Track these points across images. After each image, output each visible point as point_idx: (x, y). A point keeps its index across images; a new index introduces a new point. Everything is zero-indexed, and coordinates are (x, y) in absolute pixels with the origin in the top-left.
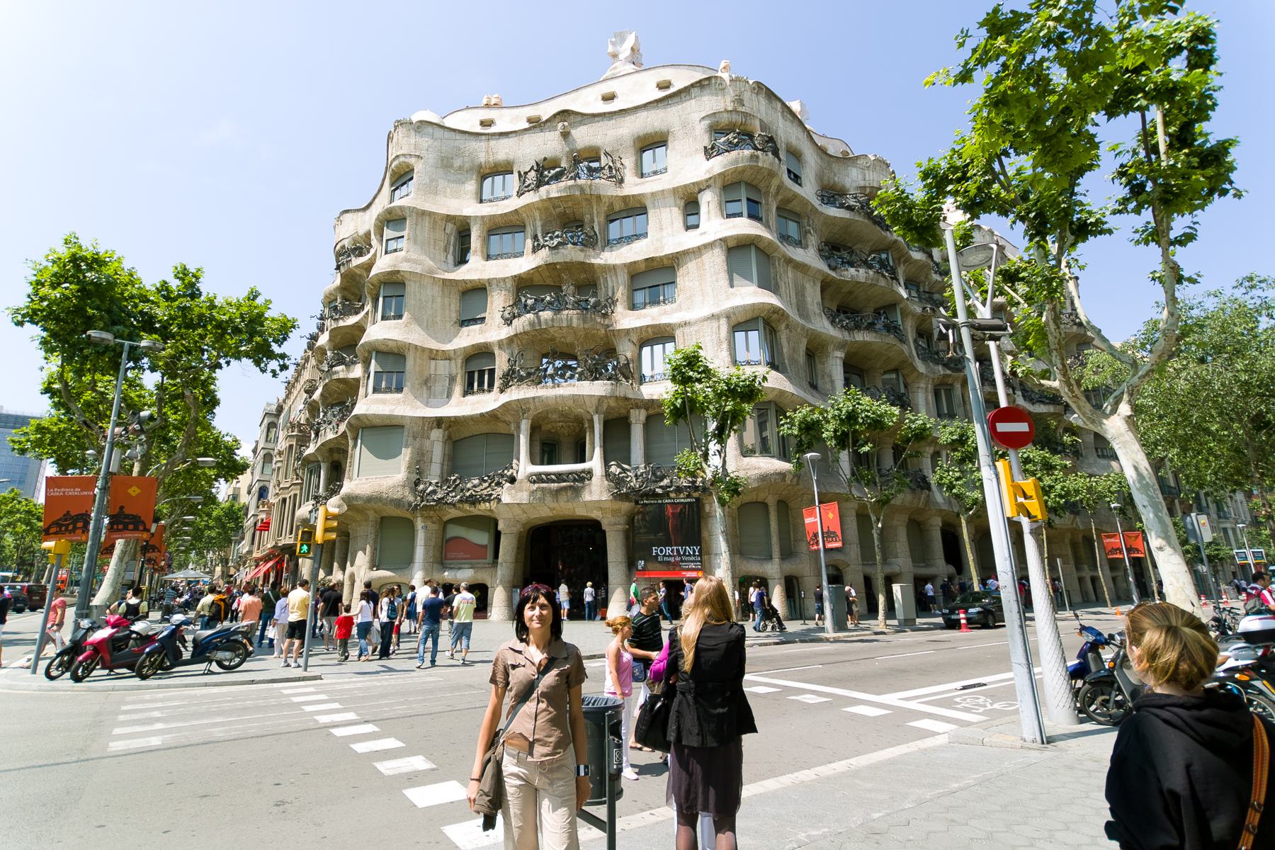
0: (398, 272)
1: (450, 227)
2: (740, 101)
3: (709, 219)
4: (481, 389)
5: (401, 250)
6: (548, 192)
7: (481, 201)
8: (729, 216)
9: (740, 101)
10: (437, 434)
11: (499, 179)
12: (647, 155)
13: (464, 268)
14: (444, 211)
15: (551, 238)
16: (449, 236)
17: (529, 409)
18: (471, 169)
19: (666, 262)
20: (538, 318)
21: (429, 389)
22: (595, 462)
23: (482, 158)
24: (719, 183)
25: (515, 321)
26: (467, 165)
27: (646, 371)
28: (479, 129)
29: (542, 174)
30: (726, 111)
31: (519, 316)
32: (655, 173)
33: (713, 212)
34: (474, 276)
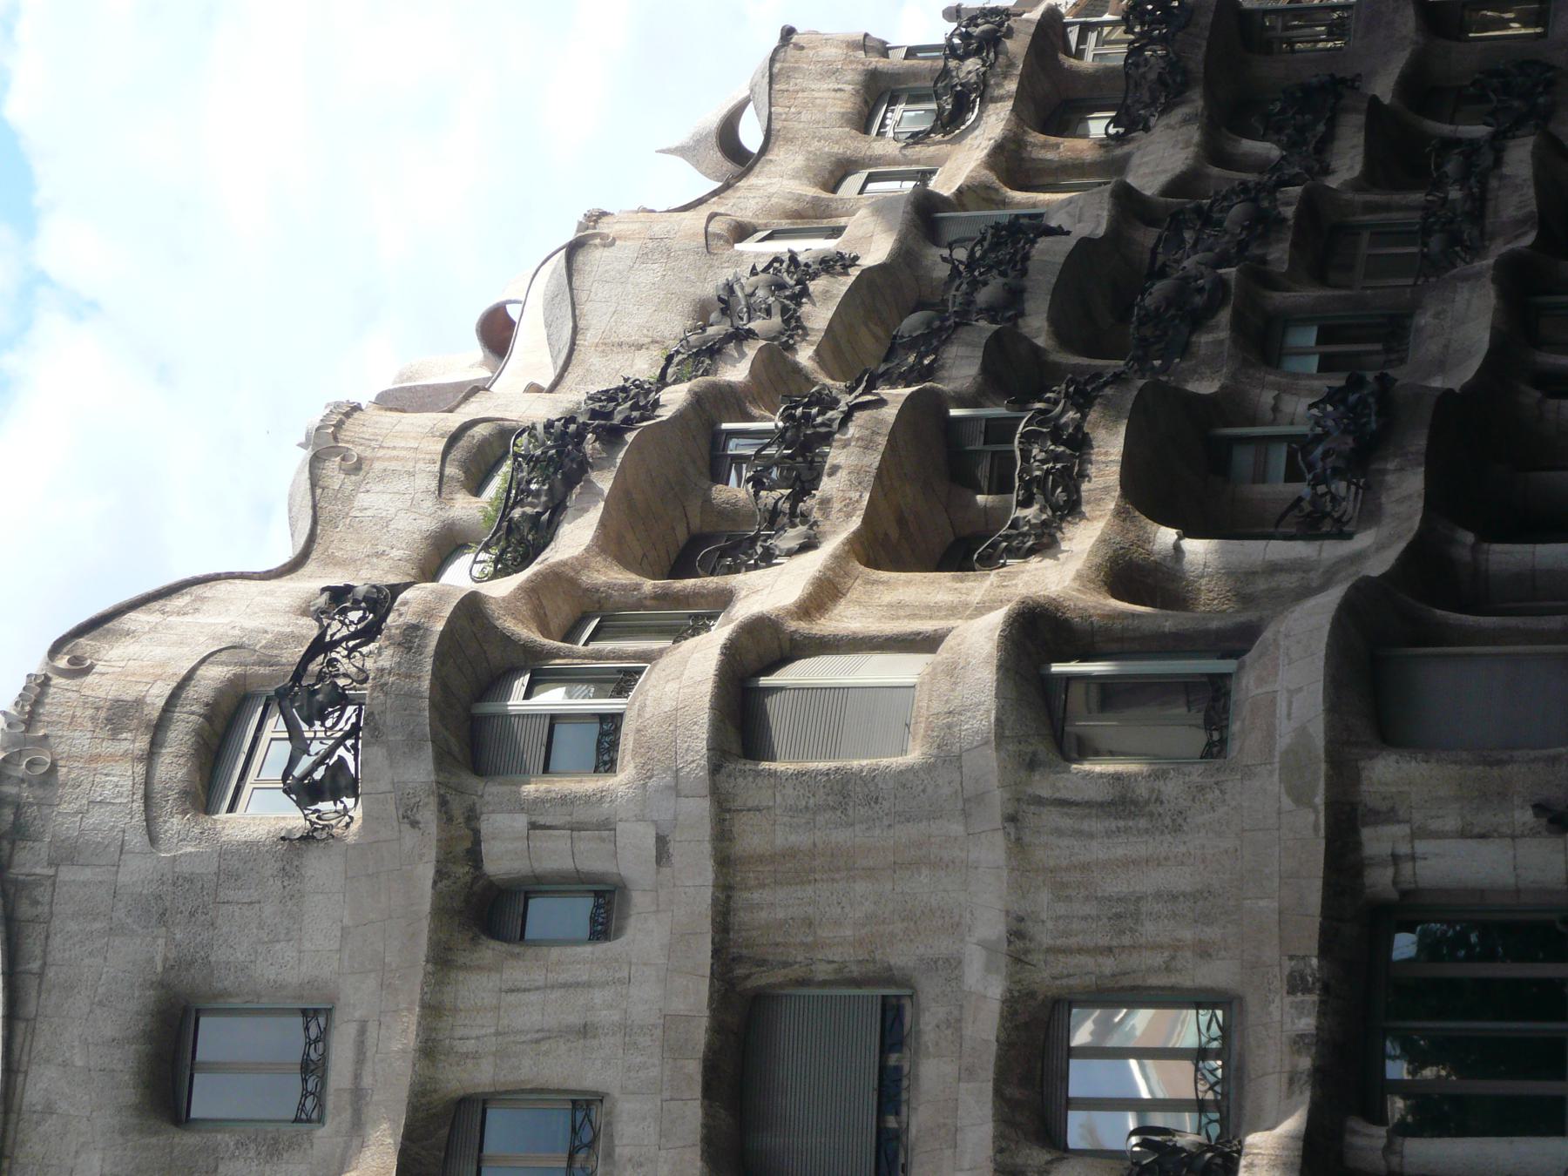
9: (118, 715)
30: (150, 756)
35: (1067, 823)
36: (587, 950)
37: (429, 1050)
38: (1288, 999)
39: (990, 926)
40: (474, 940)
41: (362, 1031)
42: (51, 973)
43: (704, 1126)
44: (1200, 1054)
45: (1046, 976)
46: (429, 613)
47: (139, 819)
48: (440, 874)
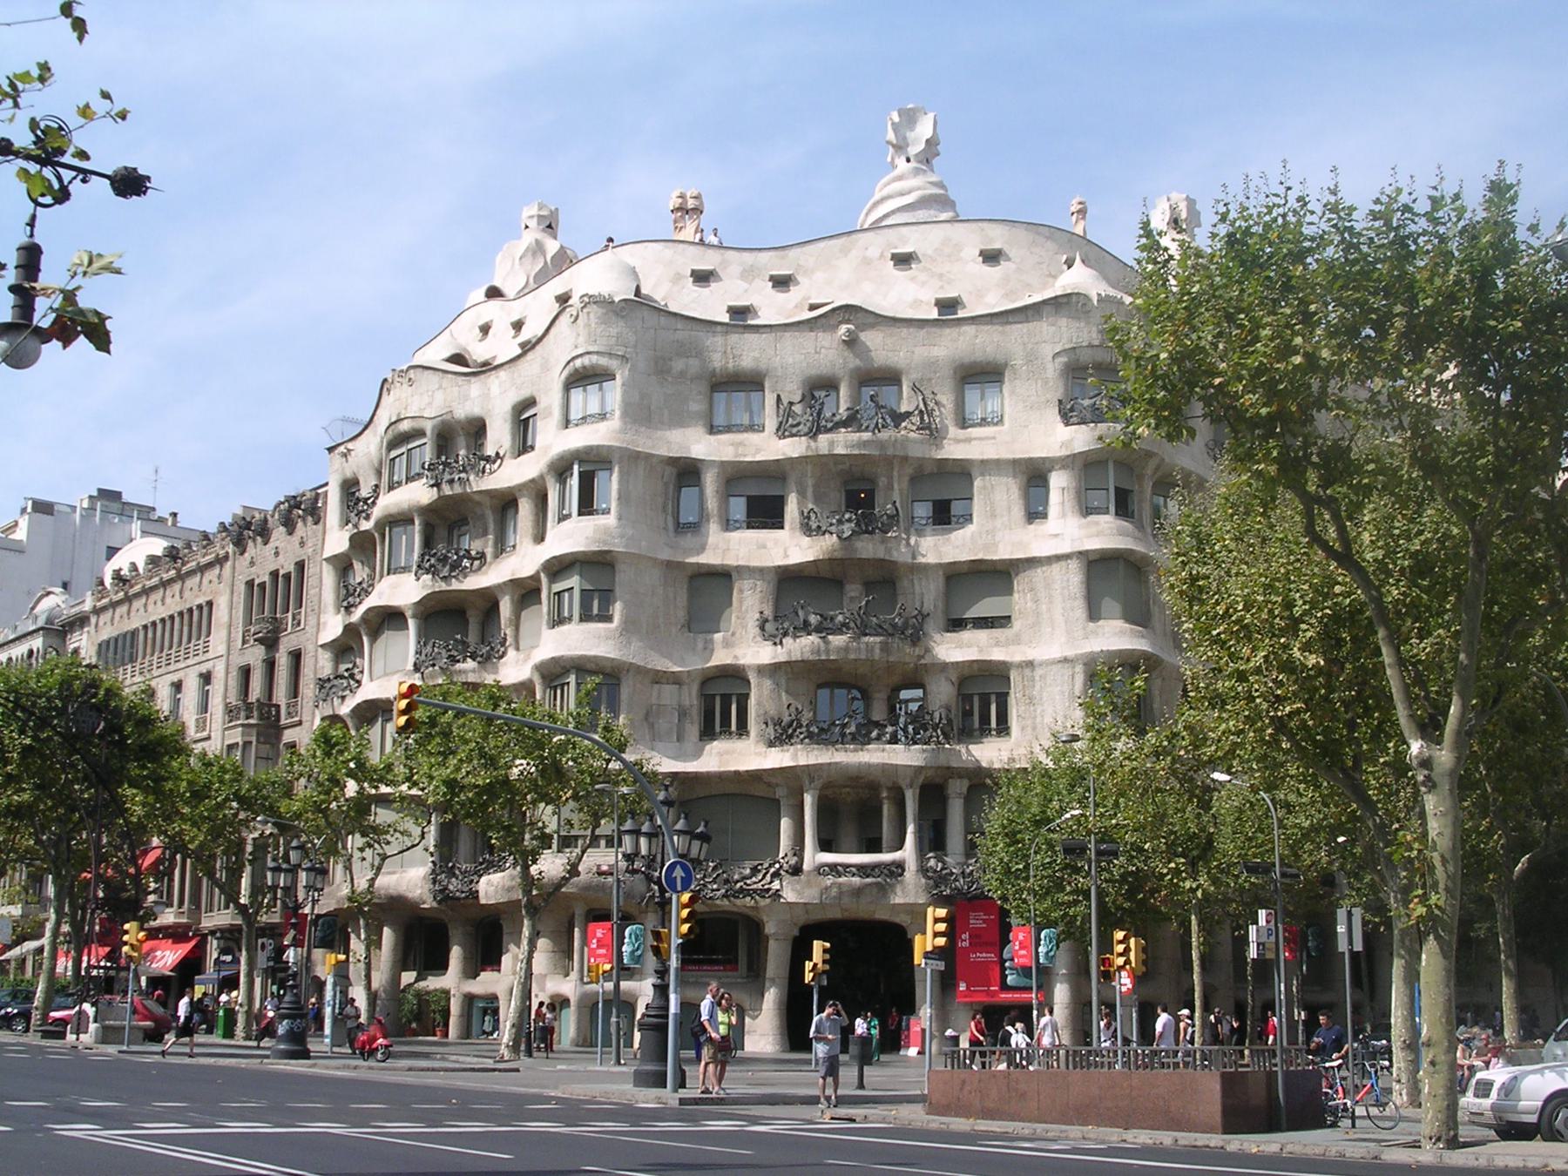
1: (670, 471)
3: (1064, 515)
6: (832, 443)
7: (712, 430)
14: (663, 451)
15: (840, 522)
16: (666, 484)
17: (820, 777)
18: (696, 378)
20: (827, 643)
21: (652, 726)
23: (717, 361)
24: (1079, 464)
25: (788, 641)
30: (1090, 346)
33: (1068, 505)
37: (982, 461)
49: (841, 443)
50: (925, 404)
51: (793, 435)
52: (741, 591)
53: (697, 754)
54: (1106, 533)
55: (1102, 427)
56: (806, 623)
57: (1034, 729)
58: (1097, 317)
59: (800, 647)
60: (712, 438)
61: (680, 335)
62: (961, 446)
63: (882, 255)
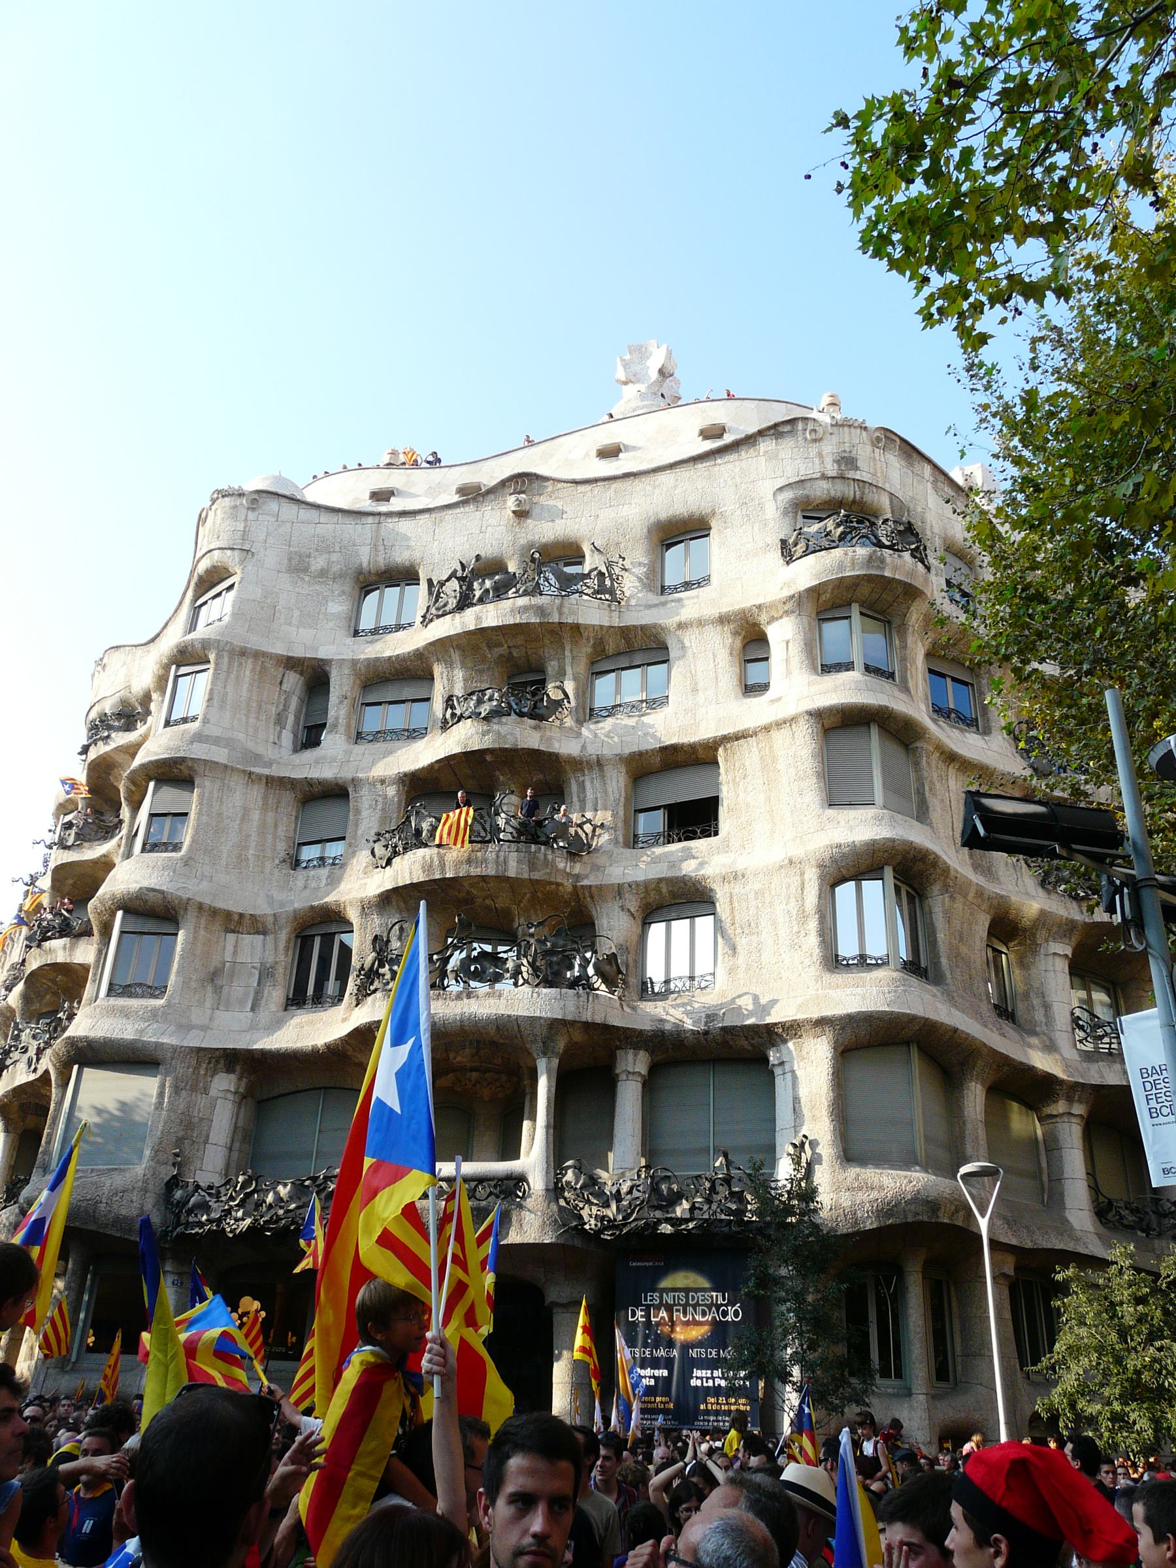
0: (183, 760)
1: (293, 681)
2: (847, 461)
4: (319, 1000)
5: (194, 719)
6: (478, 619)
7: (356, 633)
8: (827, 669)
9: (847, 461)
10: (224, 1083)
11: (392, 593)
12: (674, 555)
13: (309, 755)
14: (280, 649)
15: (480, 702)
18: (341, 575)
19: (701, 754)
21: (218, 990)
22: (532, 1156)
26: (336, 568)
27: (655, 970)
28: (367, 505)
29: (470, 588)
30: (824, 477)
31: (406, 850)
32: (687, 585)
34: (326, 773)
35: (793, 889)
36: (736, 682)
37: (681, 626)
38: (703, 1015)
39: (741, 863)
40: (735, 633)
41: (693, 598)
42: (717, 468)
43: (647, 751)
44: (692, 978)
45: (721, 895)
46: (895, 568)
47: (792, 480)
48: (759, 607)
49: (492, 615)
50: (609, 565)
51: (438, 617)
52: (358, 812)
53: (276, 1025)
54: (846, 690)
55: (837, 553)
56: (418, 832)
57: (748, 968)
58: (829, 448)
59: (410, 868)
60: (350, 641)
61: (321, 530)
62: (655, 610)
63: (587, 455)
